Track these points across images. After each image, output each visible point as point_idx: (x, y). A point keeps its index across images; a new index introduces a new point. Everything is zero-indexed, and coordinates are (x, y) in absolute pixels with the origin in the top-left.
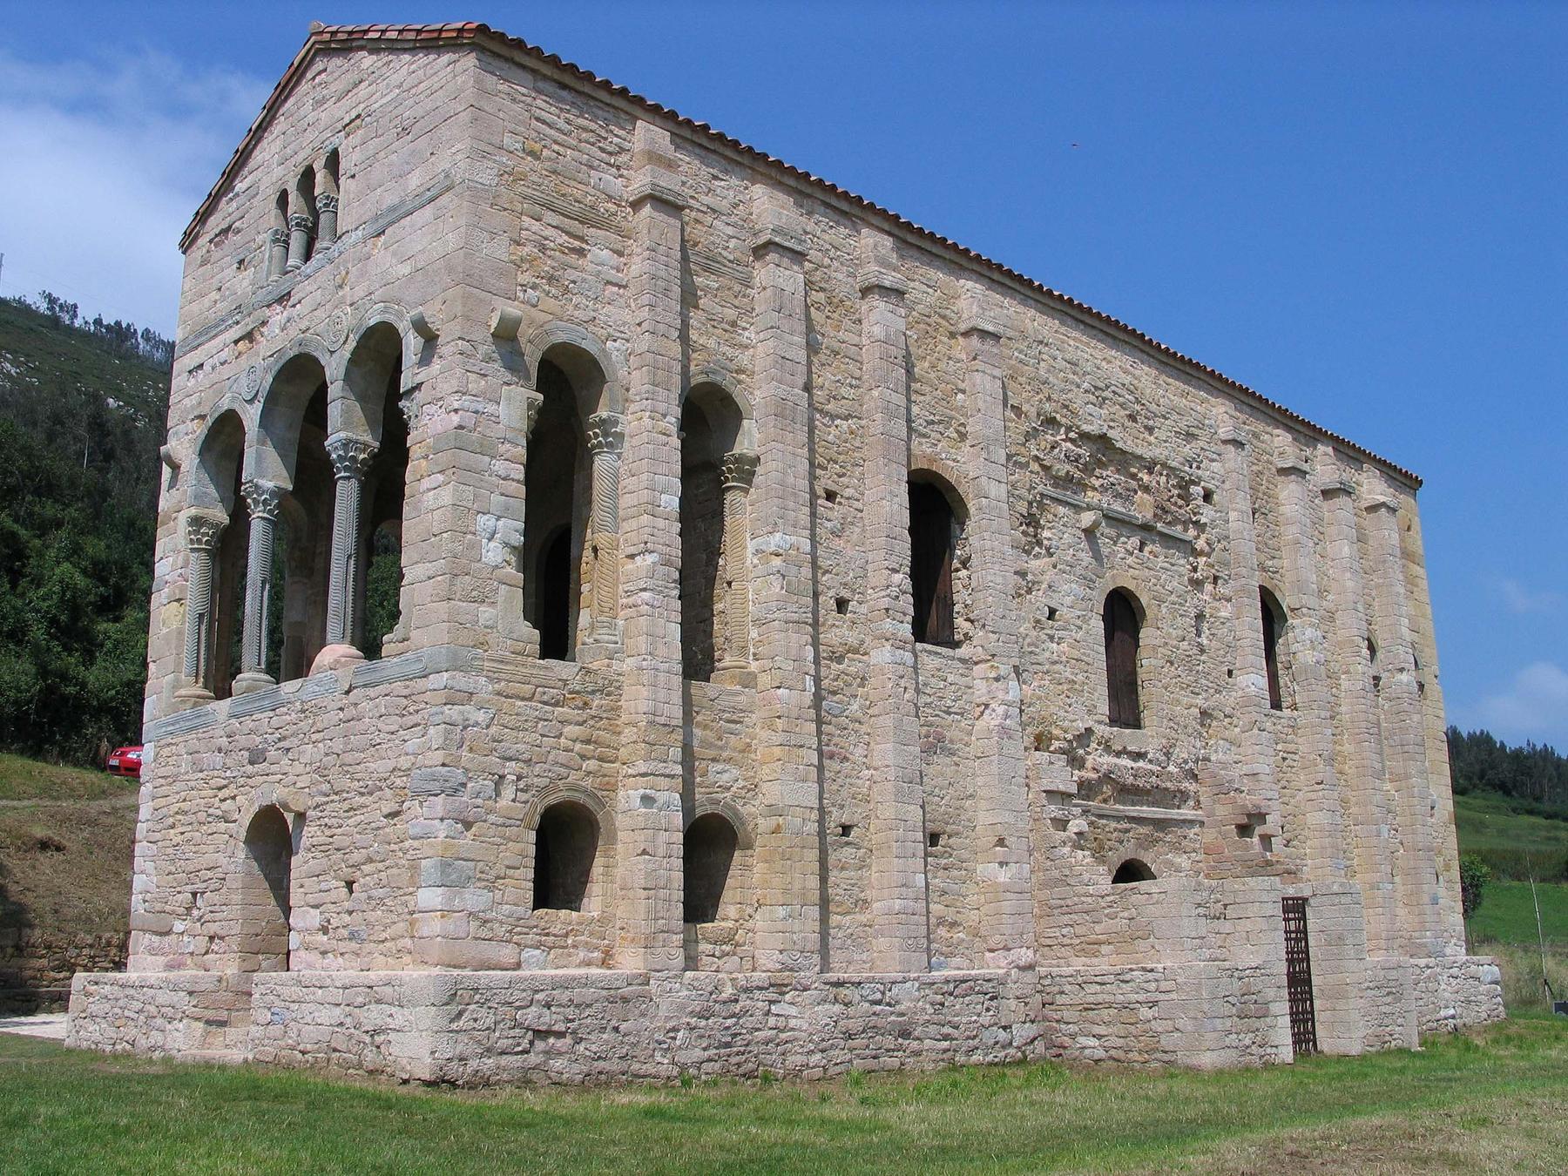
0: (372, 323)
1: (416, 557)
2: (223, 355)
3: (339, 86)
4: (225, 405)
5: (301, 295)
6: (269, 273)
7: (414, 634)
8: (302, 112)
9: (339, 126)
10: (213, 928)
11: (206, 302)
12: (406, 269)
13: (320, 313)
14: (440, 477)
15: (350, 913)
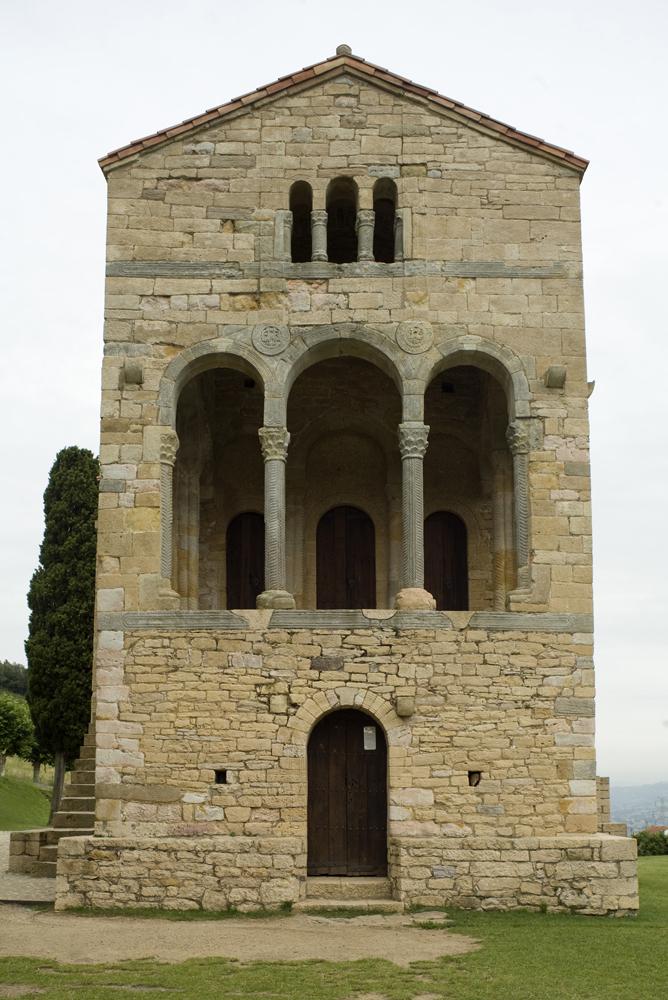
0: (467, 347)
1: (550, 546)
2: (214, 300)
3: (391, 123)
4: (222, 345)
5: (346, 288)
6: (285, 250)
7: (552, 601)
8: (324, 121)
9: (393, 160)
10: (258, 801)
11: (165, 238)
12: (508, 320)
13: (383, 314)
14: (577, 495)
15: (479, 794)
